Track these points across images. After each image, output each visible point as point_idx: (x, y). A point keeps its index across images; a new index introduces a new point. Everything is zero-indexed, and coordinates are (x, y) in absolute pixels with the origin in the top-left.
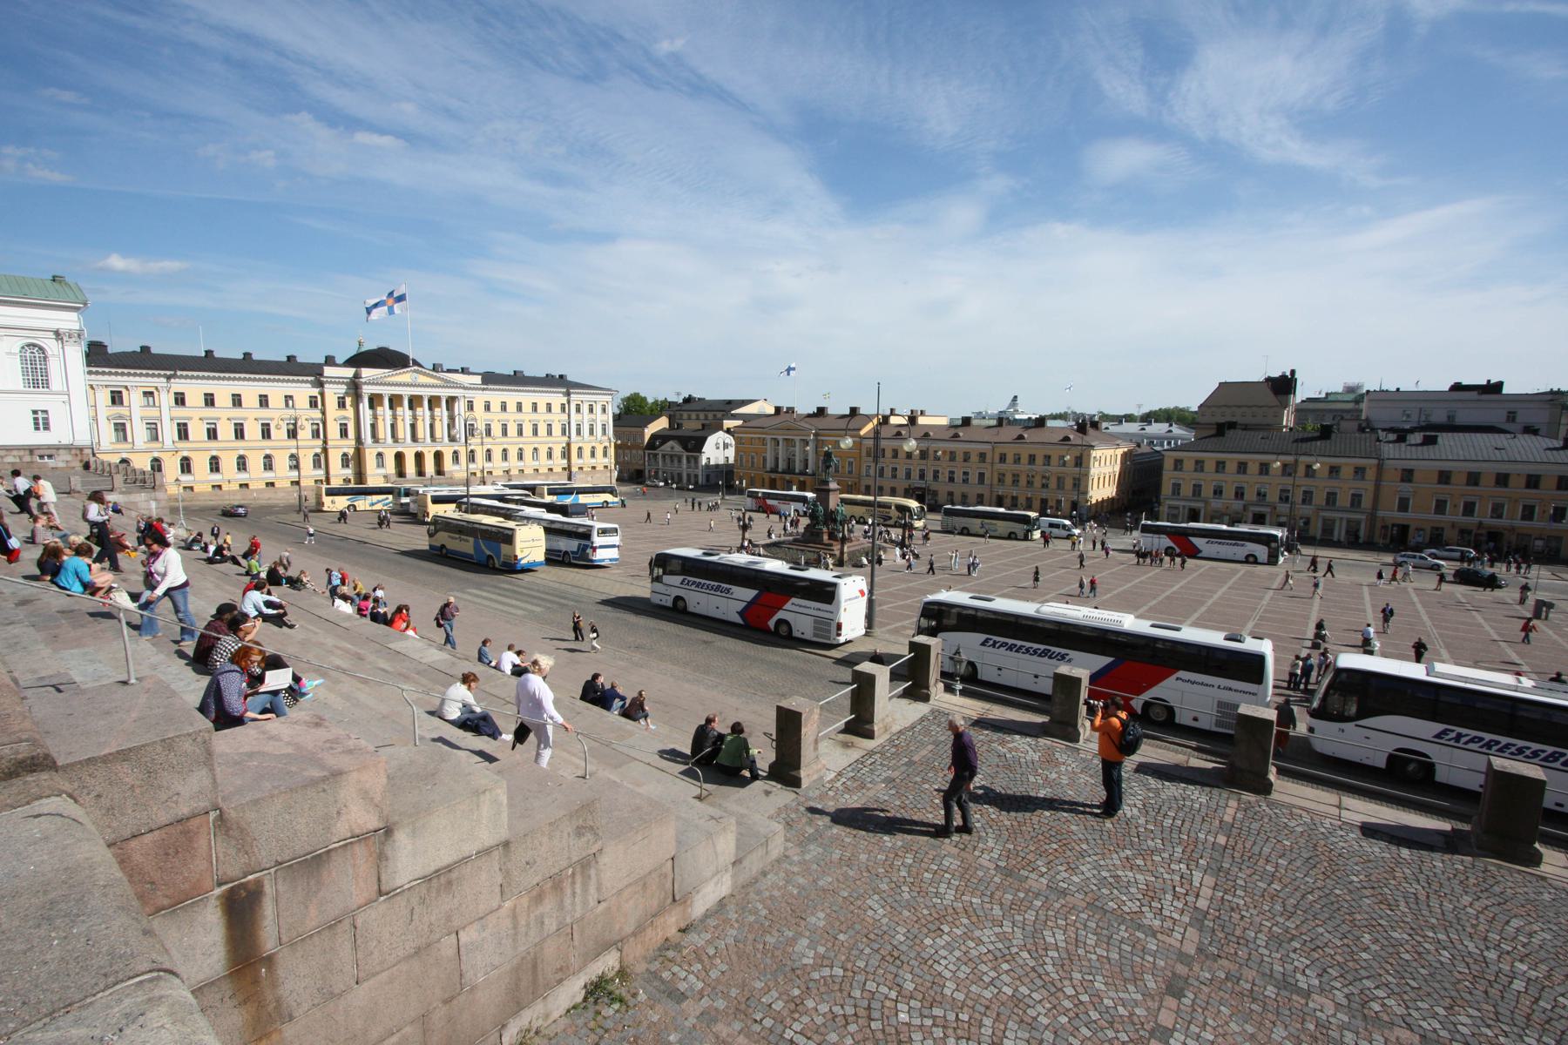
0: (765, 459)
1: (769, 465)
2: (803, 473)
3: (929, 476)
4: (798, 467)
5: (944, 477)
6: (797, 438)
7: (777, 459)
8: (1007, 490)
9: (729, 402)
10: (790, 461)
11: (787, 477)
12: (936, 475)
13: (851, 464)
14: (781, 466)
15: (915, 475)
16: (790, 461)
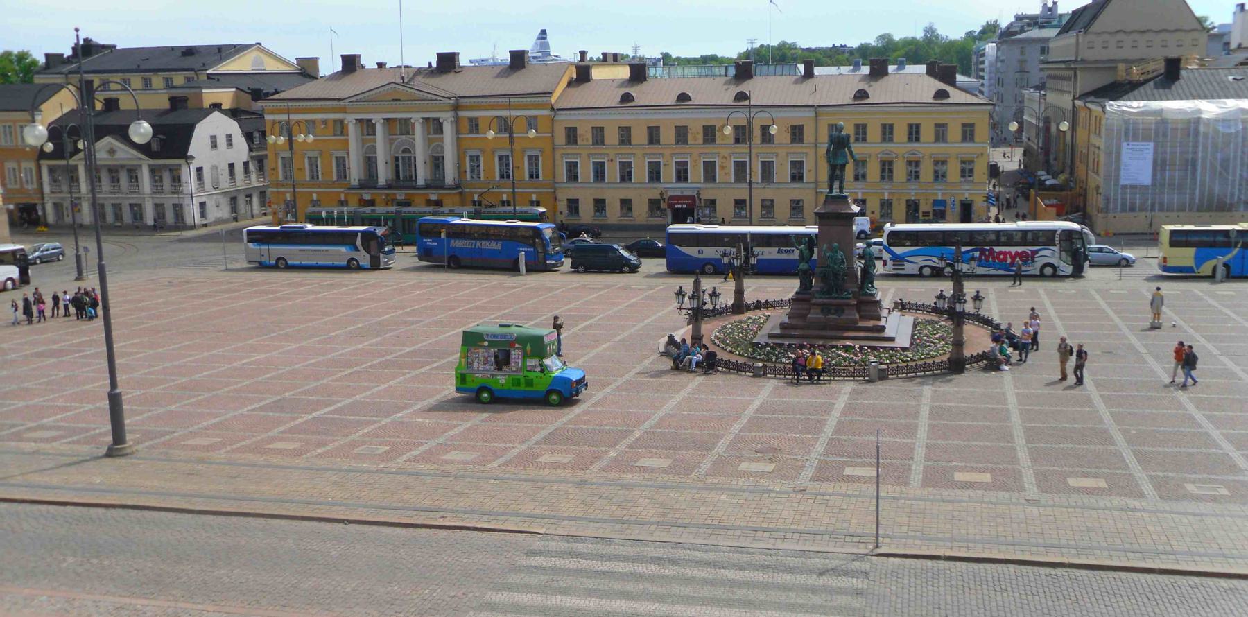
0: (342, 163)
1: (355, 173)
2: (436, 183)
3: (696, 173)
4: (422, 174)
5: (726, 173)
6: (417, 117)
7: (370, 162)
8: (926, 191)
9: (189, 52)
10: (402, 163)
11: (400, 195)
12: (710, 170)
13: (533, 160)
14: (383, 174)
15: (669, 173)
16: (402, 163)
